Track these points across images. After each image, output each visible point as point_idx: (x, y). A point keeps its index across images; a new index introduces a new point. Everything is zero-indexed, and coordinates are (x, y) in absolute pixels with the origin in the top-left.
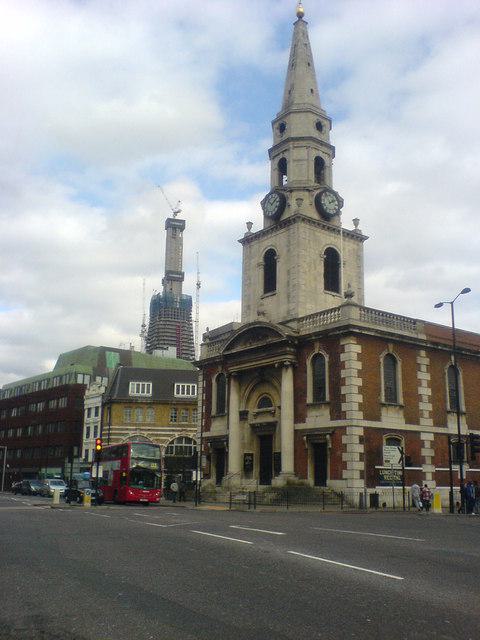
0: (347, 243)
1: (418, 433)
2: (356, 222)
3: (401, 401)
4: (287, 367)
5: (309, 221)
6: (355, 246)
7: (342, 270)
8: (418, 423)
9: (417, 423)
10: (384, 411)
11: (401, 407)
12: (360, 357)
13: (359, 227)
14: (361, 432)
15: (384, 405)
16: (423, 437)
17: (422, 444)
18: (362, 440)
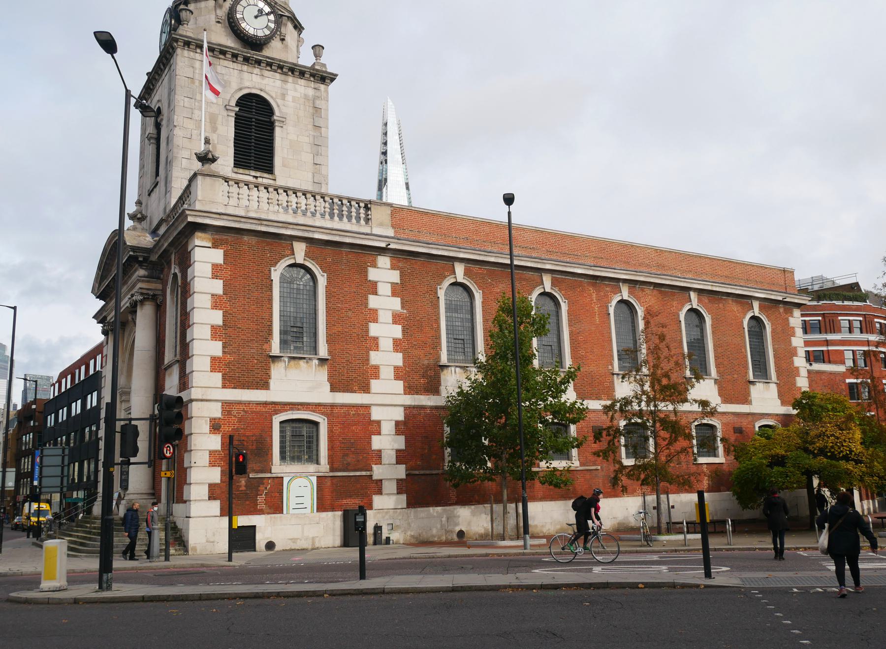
0: (290, 86)
1: (367, 407)
2: (317, 49)
3: (323, 351)
4: (142, 302)
5: (218, 51)
6: (311, 92)
7: (278, 132)
8: (366, 389)
9: (366, 389)
10: (277, 371)
11: (322, 361)
12: (217, 271)
13: (323, 60)
14: (216, 411)
15: (275, 358)
16: (376, 414)
17: (375, 427)
18: (215, 426)
